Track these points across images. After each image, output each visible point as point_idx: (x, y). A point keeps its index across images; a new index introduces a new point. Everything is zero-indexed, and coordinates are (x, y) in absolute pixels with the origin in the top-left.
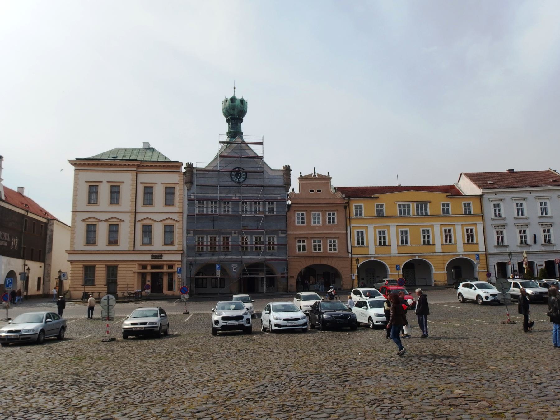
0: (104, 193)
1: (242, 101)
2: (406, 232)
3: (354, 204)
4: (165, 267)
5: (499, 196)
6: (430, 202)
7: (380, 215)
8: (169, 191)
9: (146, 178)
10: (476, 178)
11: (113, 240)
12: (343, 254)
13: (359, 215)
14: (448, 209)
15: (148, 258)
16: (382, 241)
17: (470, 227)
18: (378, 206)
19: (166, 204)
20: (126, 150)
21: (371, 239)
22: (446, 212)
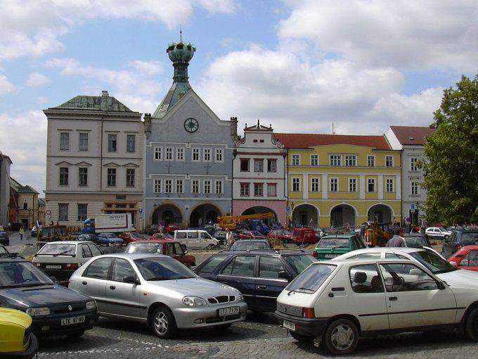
0: (74, 138)
1: (189, 47)
2: (336, 180)
3: (291, 154)
4: (128, 206)
5: (416, 152)
6: (358, 154)
7: (314, 163)
8: (131, 139)
9: (110, 126)
10: (399, 131)
11: (83, 180)
12: (282, 198)
13: (296, 163)
14: (373, 162)
15: (113, 200)
16: (315, 186)
17: (390, 178)
18: (312, 157)
19: (128, 151)
20: (87, 98)
21: (305, 185)
22: (371, 164)
